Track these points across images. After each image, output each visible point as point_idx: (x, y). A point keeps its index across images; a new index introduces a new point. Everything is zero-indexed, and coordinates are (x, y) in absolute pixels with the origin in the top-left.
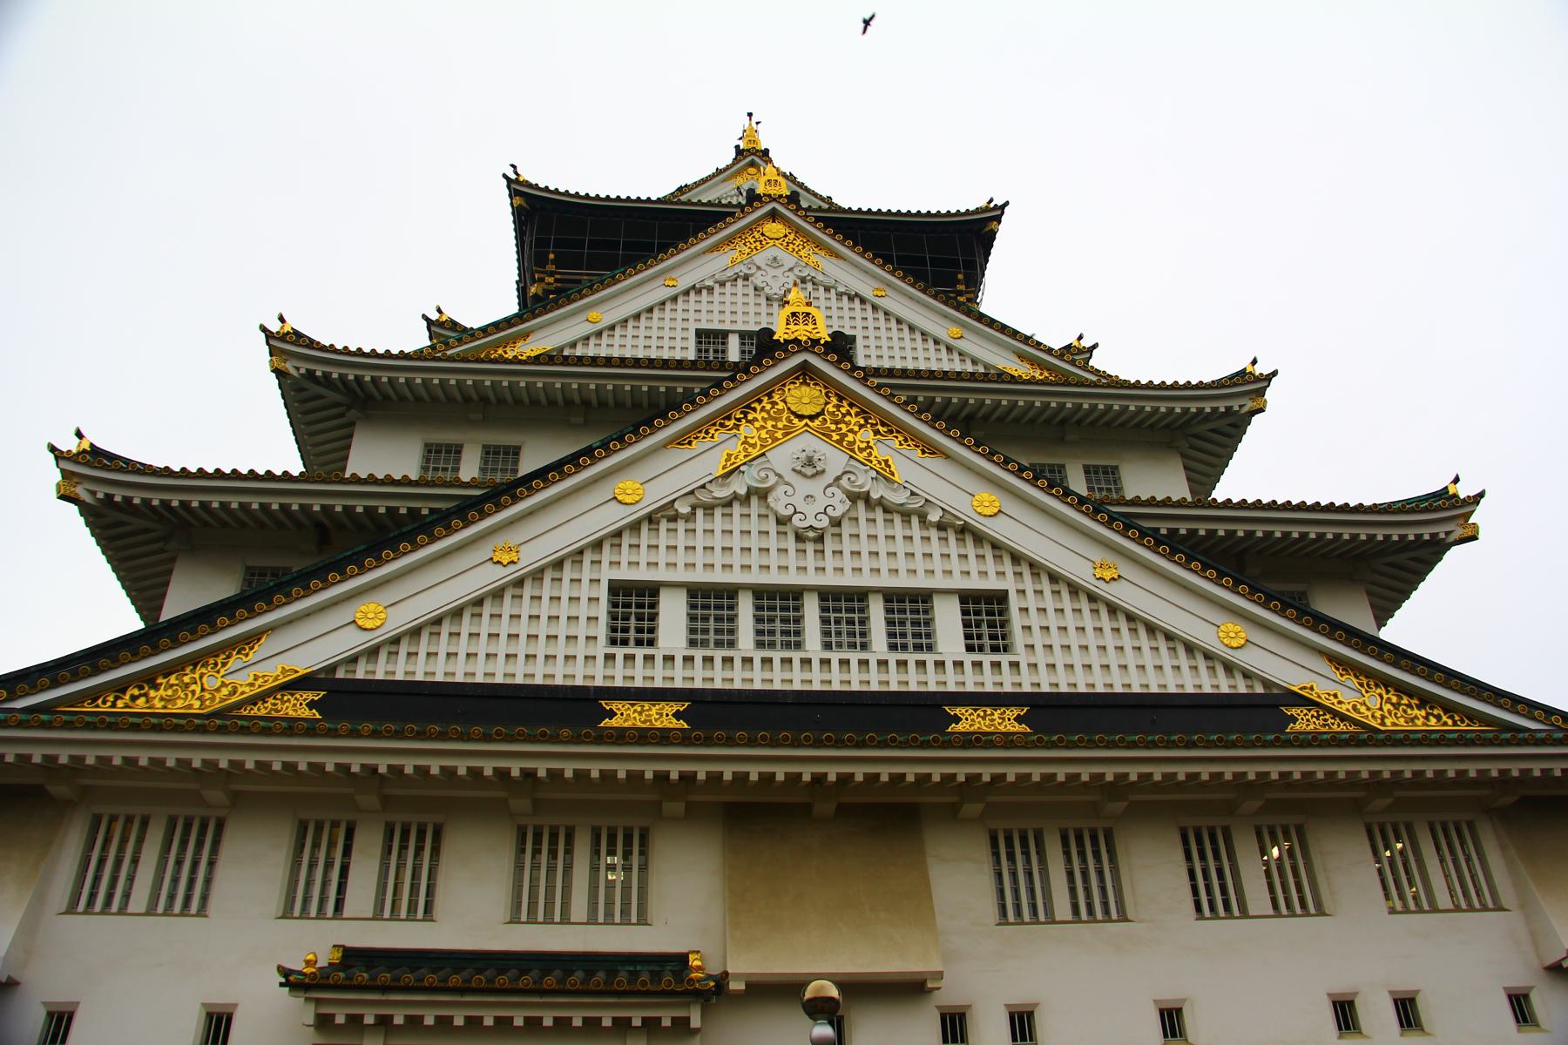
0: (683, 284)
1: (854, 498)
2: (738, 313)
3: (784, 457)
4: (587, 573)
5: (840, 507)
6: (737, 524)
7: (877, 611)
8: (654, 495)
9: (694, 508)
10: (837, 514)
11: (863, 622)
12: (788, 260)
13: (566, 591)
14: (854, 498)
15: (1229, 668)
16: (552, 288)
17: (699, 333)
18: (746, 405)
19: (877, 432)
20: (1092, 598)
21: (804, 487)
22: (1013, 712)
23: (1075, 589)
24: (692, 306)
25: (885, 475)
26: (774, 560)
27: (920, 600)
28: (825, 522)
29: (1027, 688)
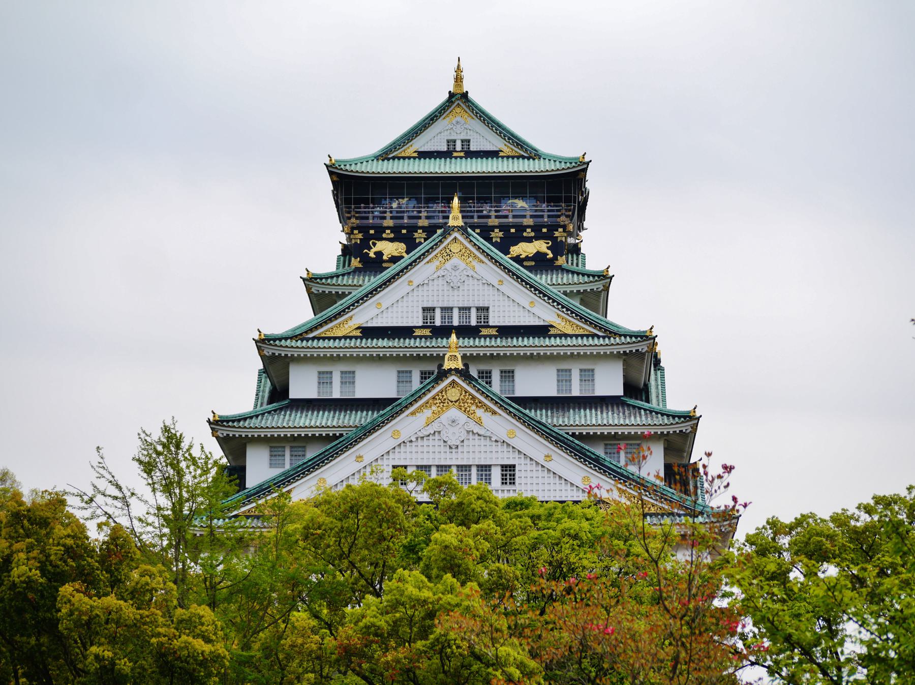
0: (415, 284)
1: (468, 432)
2: (439, 297)
4: (385, 462)
5: (464, 435)
6: (431, 443)
7: (474, 471)
8: (404, 437)
9: (417, 438)
11: (470, 475)
12: (462, 265)
14: (468, 432)
16: (355, 225)
17: (424, 309)
18: (434, 398)
19: (477, 406)
20: (543, 466)
21: (451, 430)
23: (537, 463)
24: (420, 293)
25: (479, 422)
26: (443, 455)
27: (488, 467)
28: (458, 443)
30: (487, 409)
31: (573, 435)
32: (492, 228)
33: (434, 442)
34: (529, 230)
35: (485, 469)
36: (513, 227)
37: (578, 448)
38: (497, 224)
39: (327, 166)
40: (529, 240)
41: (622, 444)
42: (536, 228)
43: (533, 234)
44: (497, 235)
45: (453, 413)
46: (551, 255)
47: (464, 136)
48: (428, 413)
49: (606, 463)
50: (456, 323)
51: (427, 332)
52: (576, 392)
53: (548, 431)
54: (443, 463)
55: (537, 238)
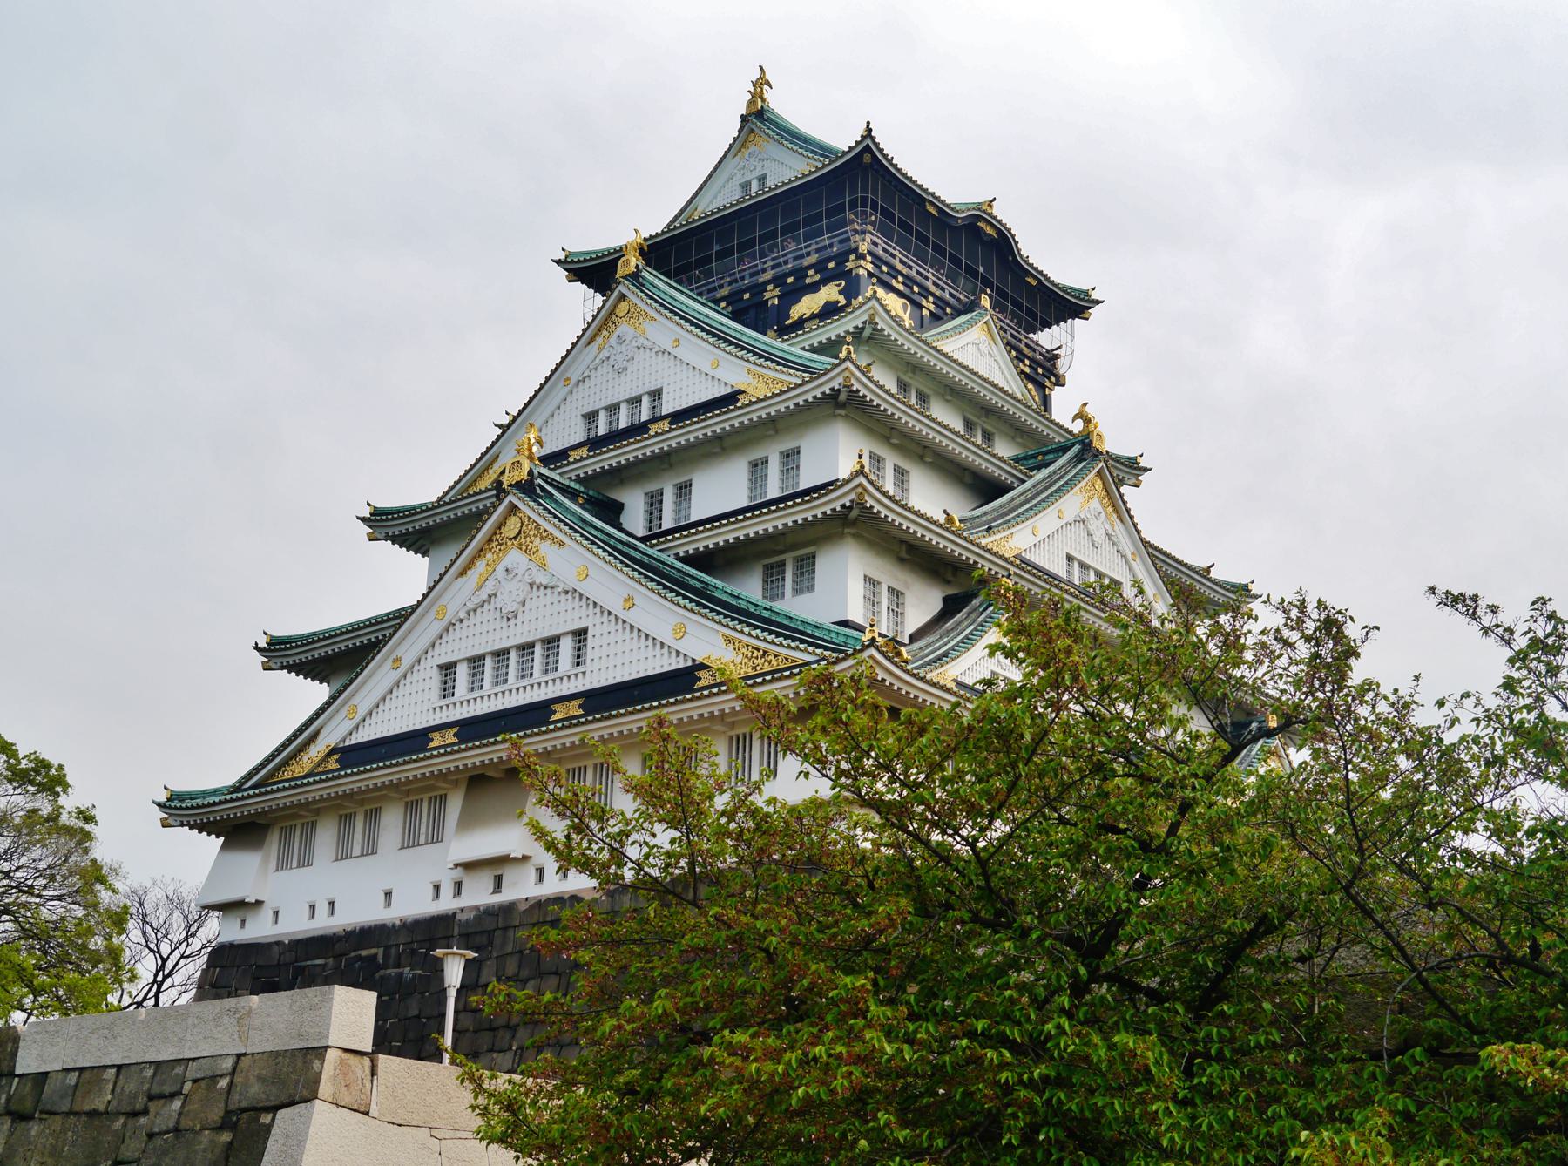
0: (573, 381)
3: (500, 570)
6: (486, 616)
9: (468, 613)
10: (520, 599)
13: (422, 675)
15: (678, 653)
17: (584, 416)
18: (490, 540)
22: (576, 703)
23: (617, 618)
25: (543, 566)
29: (588, 687)
30: (554, 540)
31: (687, 559)
32: (762, 287)
33: (486, 614)
34: (811, 272)
35: (552, 642)
36: (789, 275)
37: (677, 575)
38: (768, 276)
39: (558, 262)
40: (815, 288)
41: (789, 559)
42: (820, 267)
43: (818, 277)
44: (772, 295)
45: (514, 558)
46: (843, 302)
47: (759, 173)
48: (481, 566)
49: (718, 595)
50: (623, 425)
51: (584, 452)
52: (773, 492)
53: (638, 556)
54: (498, 646)
55: (824, 281)
